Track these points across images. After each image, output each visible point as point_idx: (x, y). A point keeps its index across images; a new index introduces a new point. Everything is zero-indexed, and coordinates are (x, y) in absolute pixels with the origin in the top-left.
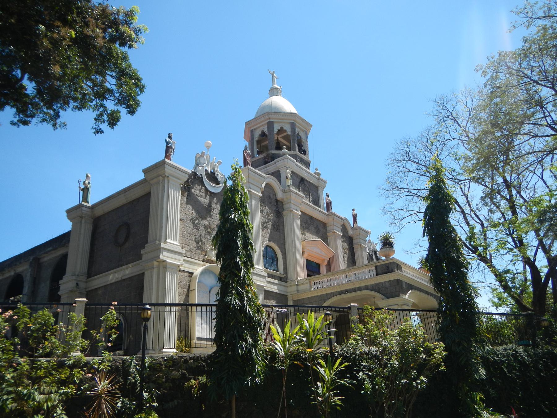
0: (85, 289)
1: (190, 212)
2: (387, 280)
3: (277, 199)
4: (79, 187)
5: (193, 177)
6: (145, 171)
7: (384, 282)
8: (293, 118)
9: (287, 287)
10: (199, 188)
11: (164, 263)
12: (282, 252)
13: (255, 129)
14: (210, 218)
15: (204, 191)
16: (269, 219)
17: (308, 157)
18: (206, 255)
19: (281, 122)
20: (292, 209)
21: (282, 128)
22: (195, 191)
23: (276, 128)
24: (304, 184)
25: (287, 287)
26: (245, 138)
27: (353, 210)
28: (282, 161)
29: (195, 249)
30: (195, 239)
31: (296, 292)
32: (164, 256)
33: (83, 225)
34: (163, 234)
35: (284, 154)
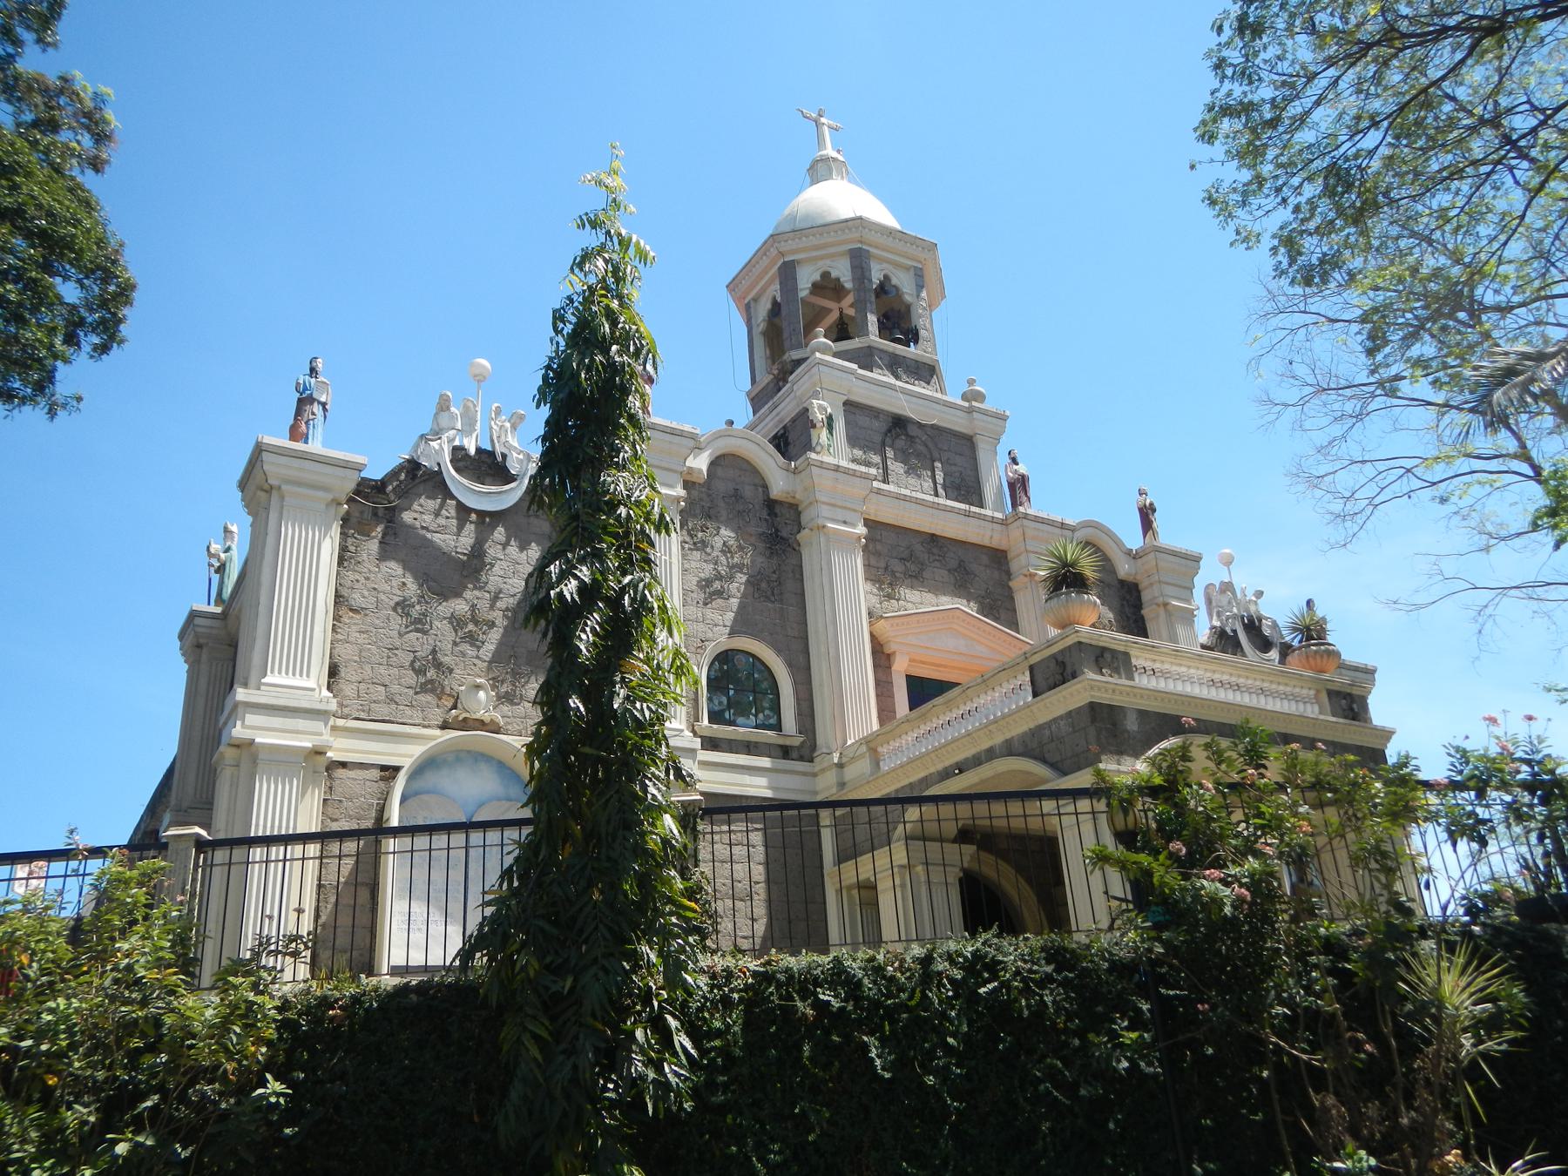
1: (394, 583)
2: (1060, 711)
3: (772, 497)
4: (210, 565)
5: (403, 476)
7: (1055, 720)
8: (856, 235)
9: (815, 775)
10: (432, 504)
12: (790, 665)
13: (755, 300)
14: (476, 593)
15: (453, 512)
16: (731, 567)
19: (822, 258)
20: (820, 522)
21: (826, 275)
22: (416, 515)
23: (806, 278)
24: (907, 435)
28: (806, 377)
29: (411, 692)
30: (413, 662)
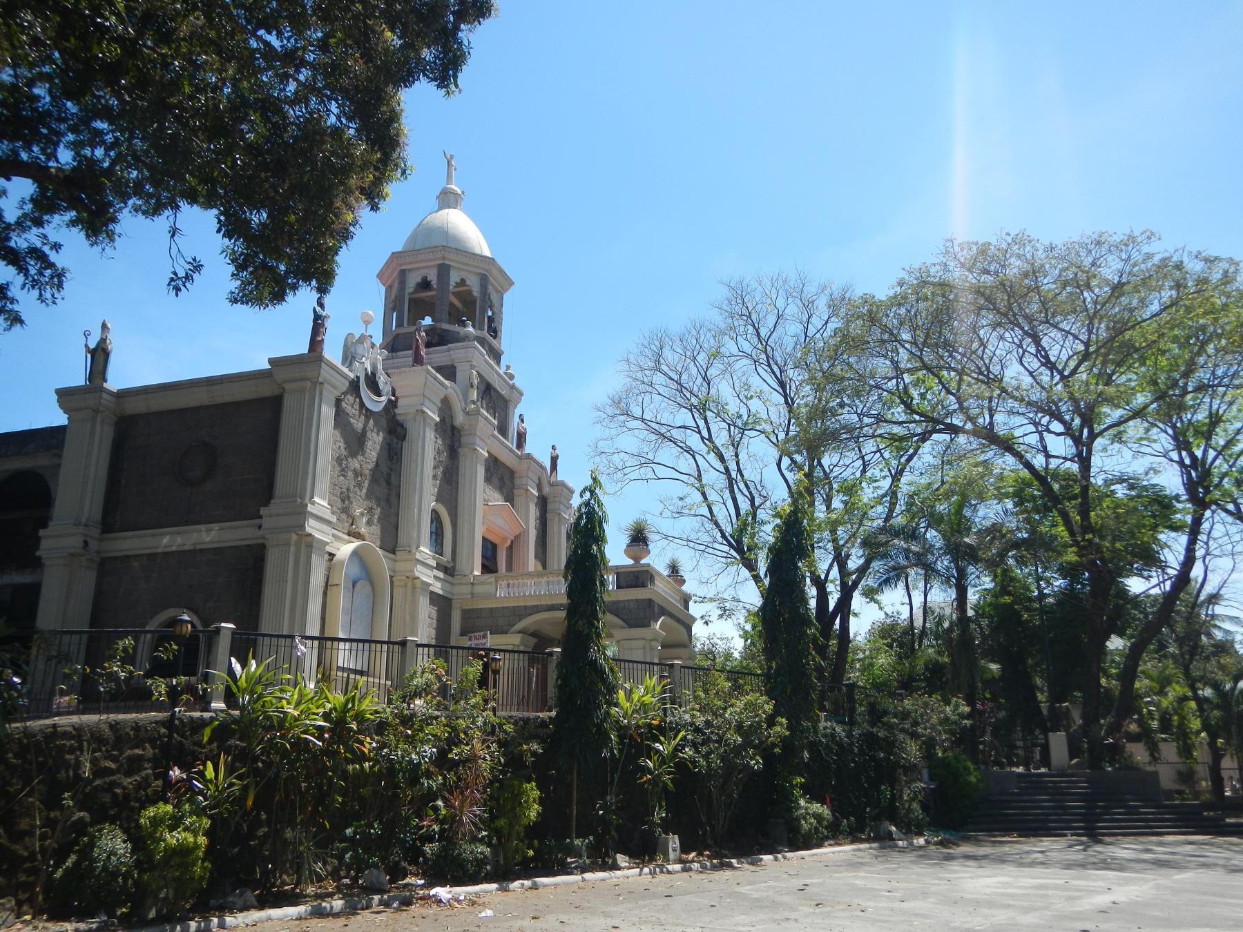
0: (98, 552)
2: (634, 598)
4: (86, 346)
6: (271, 361)
11: (309, 539)
13: (410, 270)
17: (500, 344)
18: (352, 524)
19: (463, 270)
25: (453, 584)
26: (380, 276)
27: (553, 448)
31: (470, 596)
32: (313, 527)
33: (98, 427)
34: (309, 488)
35: (466, 338)
